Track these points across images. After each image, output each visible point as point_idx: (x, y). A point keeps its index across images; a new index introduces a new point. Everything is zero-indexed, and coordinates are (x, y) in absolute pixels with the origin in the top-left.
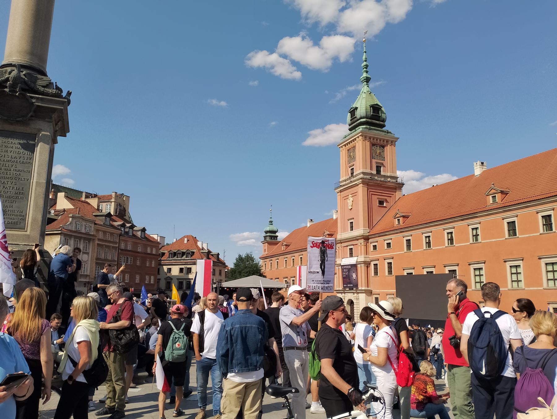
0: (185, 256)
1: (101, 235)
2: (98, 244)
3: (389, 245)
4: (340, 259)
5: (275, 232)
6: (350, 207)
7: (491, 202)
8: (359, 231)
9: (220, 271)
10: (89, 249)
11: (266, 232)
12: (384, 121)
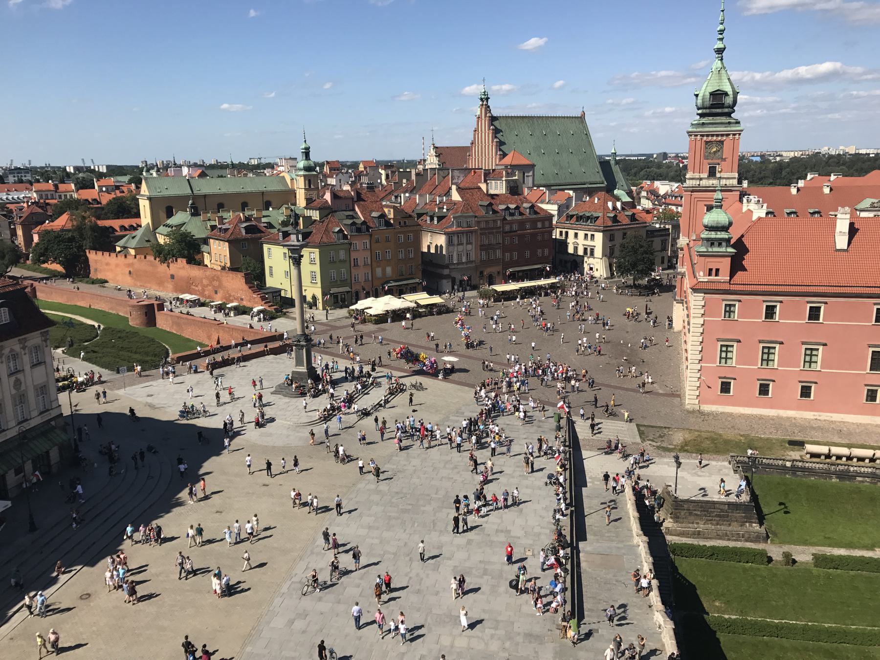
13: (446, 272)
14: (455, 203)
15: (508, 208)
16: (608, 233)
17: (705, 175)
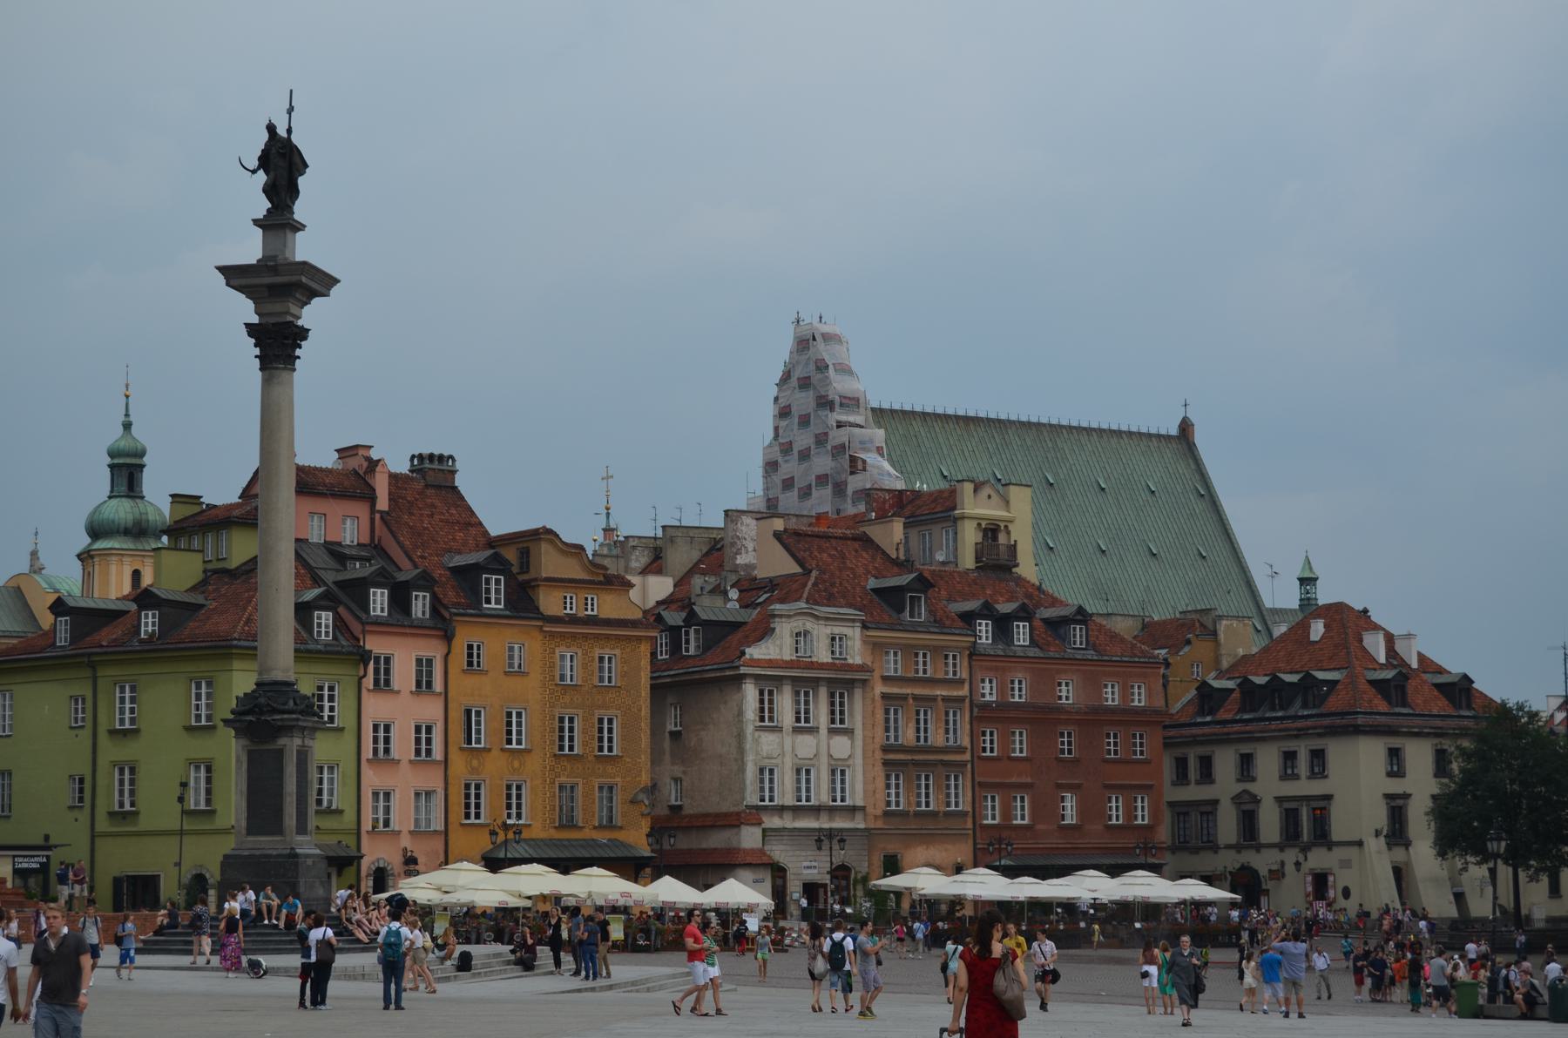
0: (1298, 703)
1: (892, 665)
2: (885, 696)
10: (851, 715)
13: (749, 838)
14: (771, 585)
15: (987, 611)
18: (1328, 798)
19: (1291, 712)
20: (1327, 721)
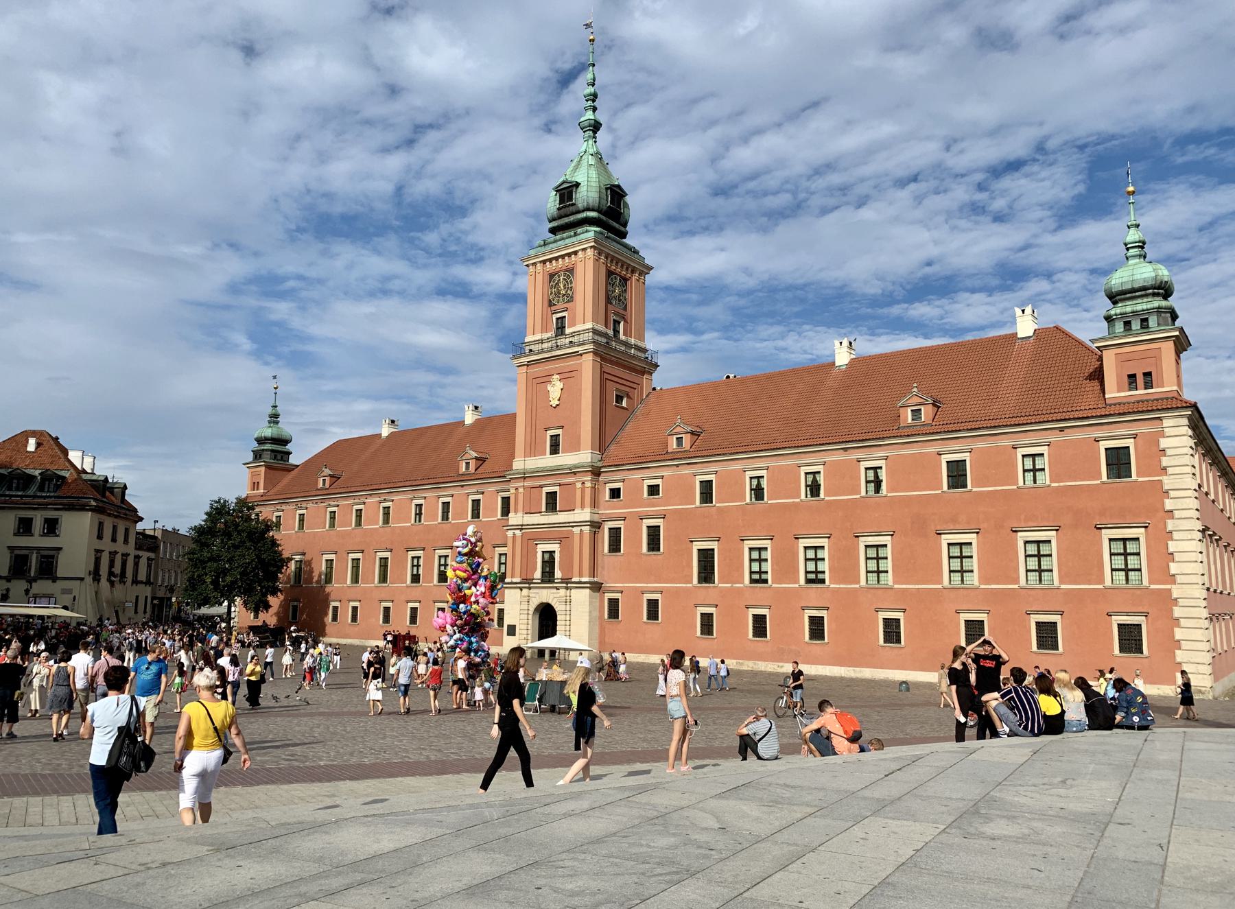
3: (654, 490)
4: (520, 514)
5: (285, 442)
6: (555, 403)
7: (910, 421)
8: (584, 456)
9: (127, 530)
11: (261, 441)
12: (625, 225)
16: (98, 516)
17: (611, 333)
18: (60, 549)
19: (30, 492)
20: (65, 501)
